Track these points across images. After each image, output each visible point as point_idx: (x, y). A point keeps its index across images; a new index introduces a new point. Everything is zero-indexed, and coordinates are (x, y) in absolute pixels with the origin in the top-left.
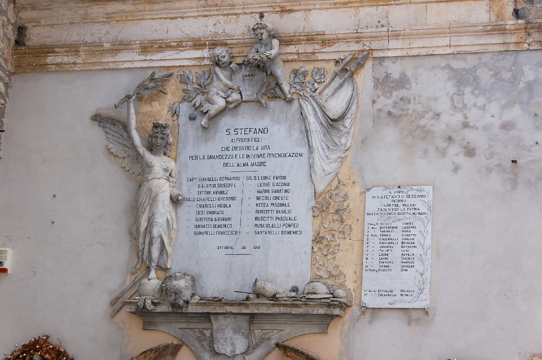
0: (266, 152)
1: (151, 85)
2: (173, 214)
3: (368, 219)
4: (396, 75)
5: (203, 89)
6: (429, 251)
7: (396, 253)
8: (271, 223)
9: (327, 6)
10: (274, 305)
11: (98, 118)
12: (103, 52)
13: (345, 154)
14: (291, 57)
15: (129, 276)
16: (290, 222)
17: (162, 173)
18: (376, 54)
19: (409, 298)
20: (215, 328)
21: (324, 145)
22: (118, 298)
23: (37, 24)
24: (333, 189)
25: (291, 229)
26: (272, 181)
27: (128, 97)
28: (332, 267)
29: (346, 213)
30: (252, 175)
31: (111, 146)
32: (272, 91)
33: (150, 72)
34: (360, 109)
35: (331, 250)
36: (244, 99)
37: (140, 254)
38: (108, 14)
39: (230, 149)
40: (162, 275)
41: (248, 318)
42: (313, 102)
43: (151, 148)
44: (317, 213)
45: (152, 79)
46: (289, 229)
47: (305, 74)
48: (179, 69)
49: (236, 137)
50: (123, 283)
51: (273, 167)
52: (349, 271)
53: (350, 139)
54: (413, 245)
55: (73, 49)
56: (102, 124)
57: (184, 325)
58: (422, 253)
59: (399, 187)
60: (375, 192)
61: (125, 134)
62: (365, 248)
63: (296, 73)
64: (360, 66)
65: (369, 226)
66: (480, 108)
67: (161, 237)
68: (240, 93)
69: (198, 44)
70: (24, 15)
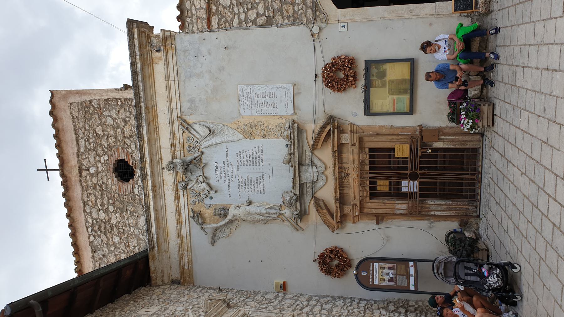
0: (226, 163)
1: (196, 218)
2: (255, 204)
3: (254, 114)
4: (189, 104)
5: (198, 194)
6: (267, 85)
7: (268, 100)
8: (258, 158)
9: (158, 138)
10: (294, 154)
11: (213, 243)
12: (182, 241)
14: (182, 154)
15: (284, 223)
16: (257, 150)
17: (236, 210)
18: (179, 115)
19: (289, 94)
20: (305, 181)
21: (222, 136)
22: (295, 228)
23: (170, 274)
25: (260, 149)
26: (239, 159)
27: (202, 228)
29: (252, 124)
30: (236, 168)
31: (225, 236)
32: (198, 161)
33: (191, 219)
36: (202, 174)
37: (274, 219)
38: (165, 241)
39: (225, 179)
40: (283, 207)
41: (301, 166)
42: (202, 142)
43: (225, 216)
44: (253, 137)
45: (193, 218)
46: (260, 150)
47: (190, 147)
48: (189, 206)
49: (220, 177)
50: (288, 226)
51: (233, 159)
52: (278, 122)
53: (219, 124)
55: (181, 256)
56: (216, 241)
57: (306, 196)
60: (242, 111)
61: (220, 229)
62: (267, 115)
63: (189, 151)
64: (185, 121)
66: (202, 65)
67: (266, 209)
68: (199, 176)
69: (177, 197)
70: (166, 281)
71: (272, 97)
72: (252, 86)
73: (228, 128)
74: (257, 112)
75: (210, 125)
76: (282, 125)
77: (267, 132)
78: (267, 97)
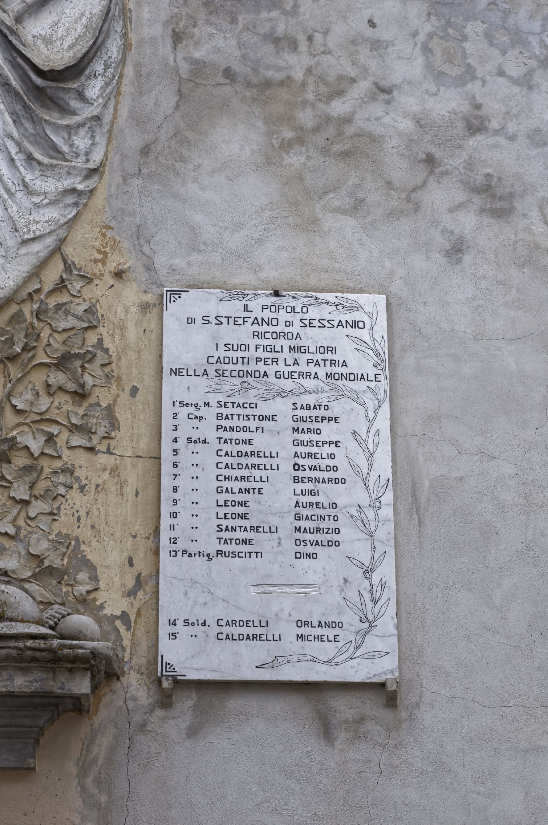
6: (388, 497)
13: (87, 183)
21: (13, 150)
24: (47, 288)
28: (45, 544)
29: (95, 368)
34: (132, 55)
35: (42, 486)
53: (101, 140)
54: (332, 475)
58: (365, 501)
59: (277, 294)
65: (178, 409)
66: (516, 82)
71: (303, 524)
72: (383, 386)
73: (70, 199)
74: (183, 412)
75: (99, 83)
76: (81, 589)
77: (27, 469)
78: (300, 487)
